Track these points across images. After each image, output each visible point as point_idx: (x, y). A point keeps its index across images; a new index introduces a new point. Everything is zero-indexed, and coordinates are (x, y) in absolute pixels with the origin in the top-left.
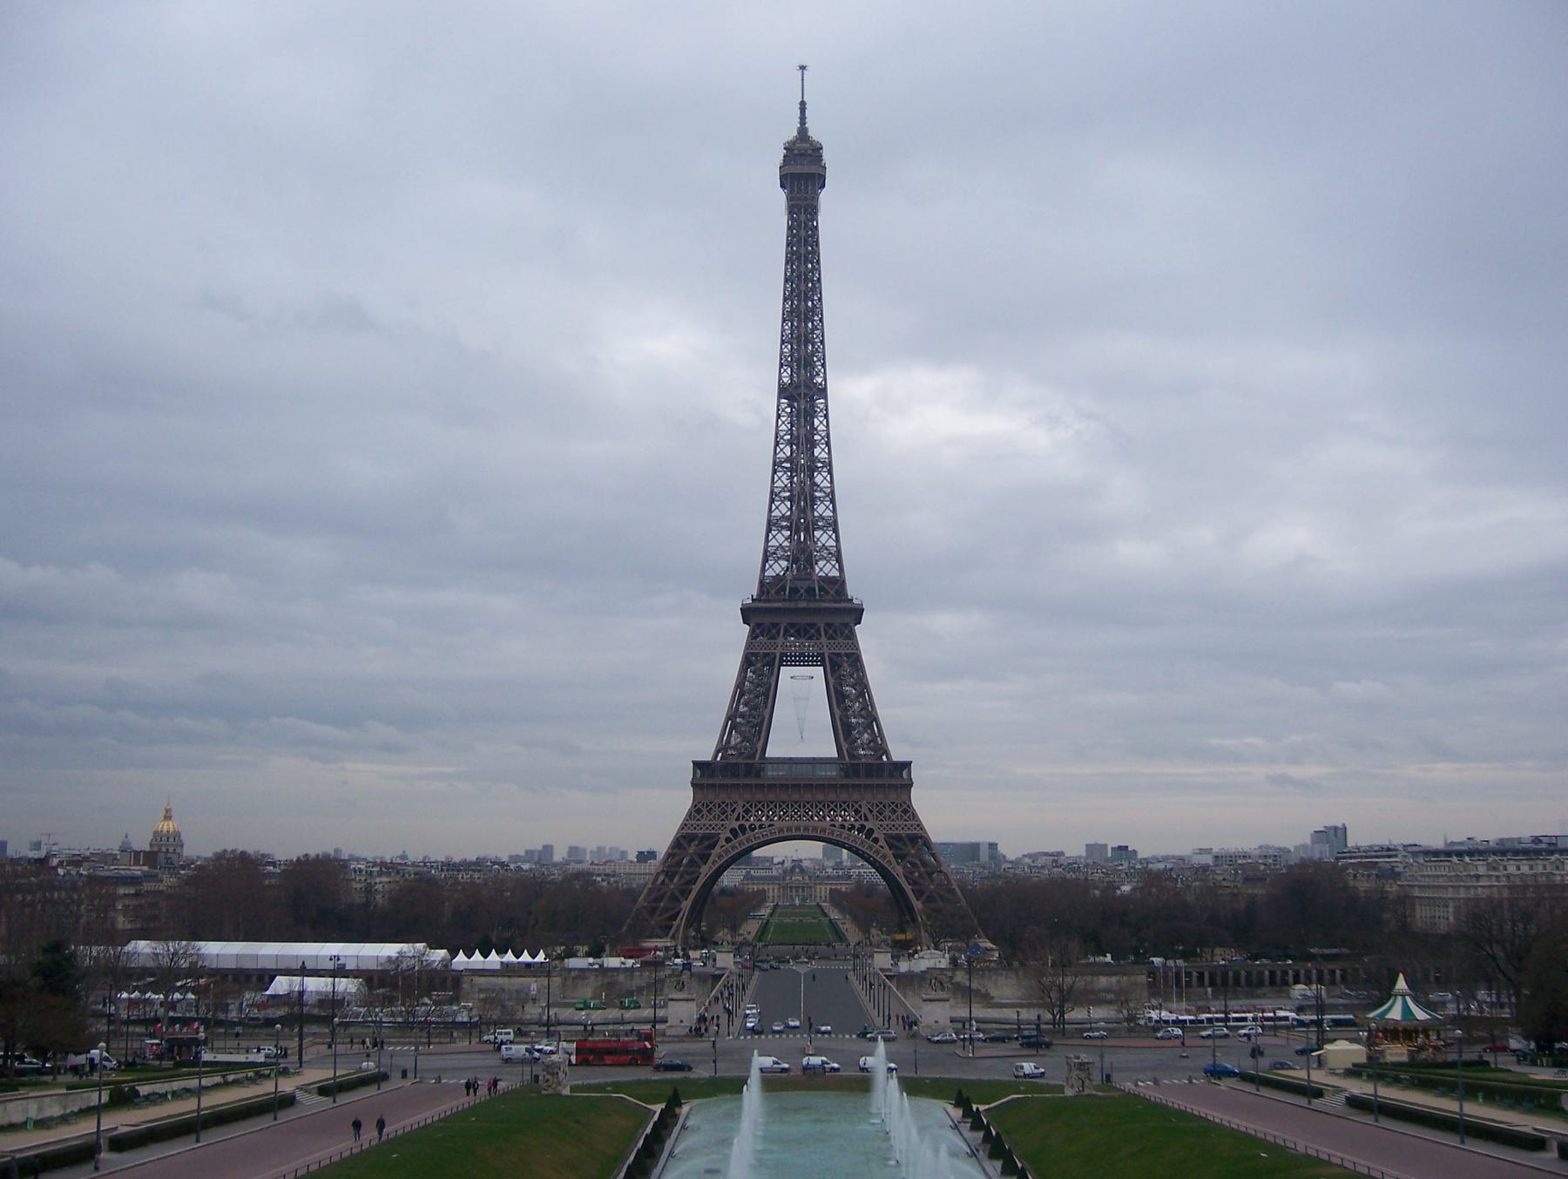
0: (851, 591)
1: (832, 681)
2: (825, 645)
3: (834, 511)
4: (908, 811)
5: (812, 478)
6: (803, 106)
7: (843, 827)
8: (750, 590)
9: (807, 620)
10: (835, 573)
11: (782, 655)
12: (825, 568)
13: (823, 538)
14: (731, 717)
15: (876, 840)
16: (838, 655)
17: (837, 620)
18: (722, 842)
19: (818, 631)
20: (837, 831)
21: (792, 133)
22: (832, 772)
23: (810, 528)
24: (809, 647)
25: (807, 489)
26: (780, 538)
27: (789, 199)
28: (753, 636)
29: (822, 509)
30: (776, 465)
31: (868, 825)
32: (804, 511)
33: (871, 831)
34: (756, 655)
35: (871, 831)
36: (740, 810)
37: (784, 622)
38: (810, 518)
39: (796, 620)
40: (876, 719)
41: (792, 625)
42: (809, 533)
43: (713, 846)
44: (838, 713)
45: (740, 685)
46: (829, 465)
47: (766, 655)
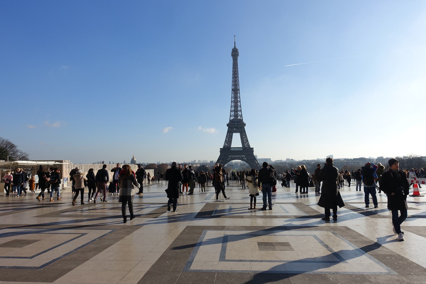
6: (235, 42)
12: (239, 118)
13: (239, 113)
14: (226, 141)
17: (242, 126)
21: (233, 47)
22: (241, 149)
23: (237, 111)
26: (233, 113)
27: (233, 58)
28: (229, 129)
29: (239, 109)
30: (232, 102)
42: (237, 112)
45: (227, 136)
46: (240, 101)
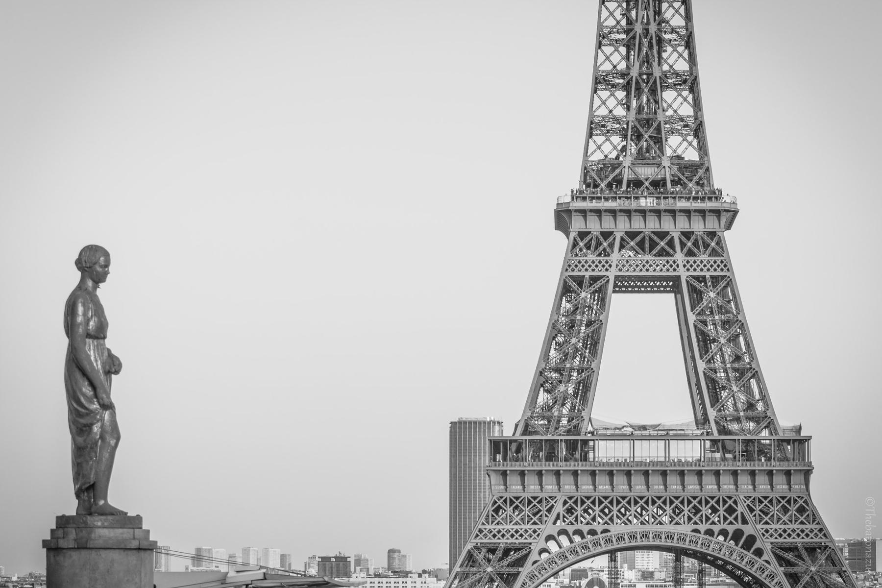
0: (718, 182)
1: (692, 318)
2: (681, 265)
3: (692, 60)
4: (805, 510)
5: (658, 12)
7: (710, 532)
8: (568, 181)
9: (653, 224)
10: (691, 155)
11: (617, 278)
12: (679, 146)
13: (675, 102)
15: (759, 553)
16: (701, 279)
17: (698, 226)
18: (534, 556)
19: (671, 244)
20: (702, 536)
24: (657, 266)
25: (653, 28)
29: (674, 60)
31: (748, 530)
32: (647, 61)
33: (751, 540)
34: (580, 281)
35: (751, 540)
36: (559, 508)
37: (622, 226)
38: (657, 73)
39: (637, 224)
40: (756, 375)
41: (632, 235)
43: (520, 562)
44: (701, 366)
47: (594, 279)
